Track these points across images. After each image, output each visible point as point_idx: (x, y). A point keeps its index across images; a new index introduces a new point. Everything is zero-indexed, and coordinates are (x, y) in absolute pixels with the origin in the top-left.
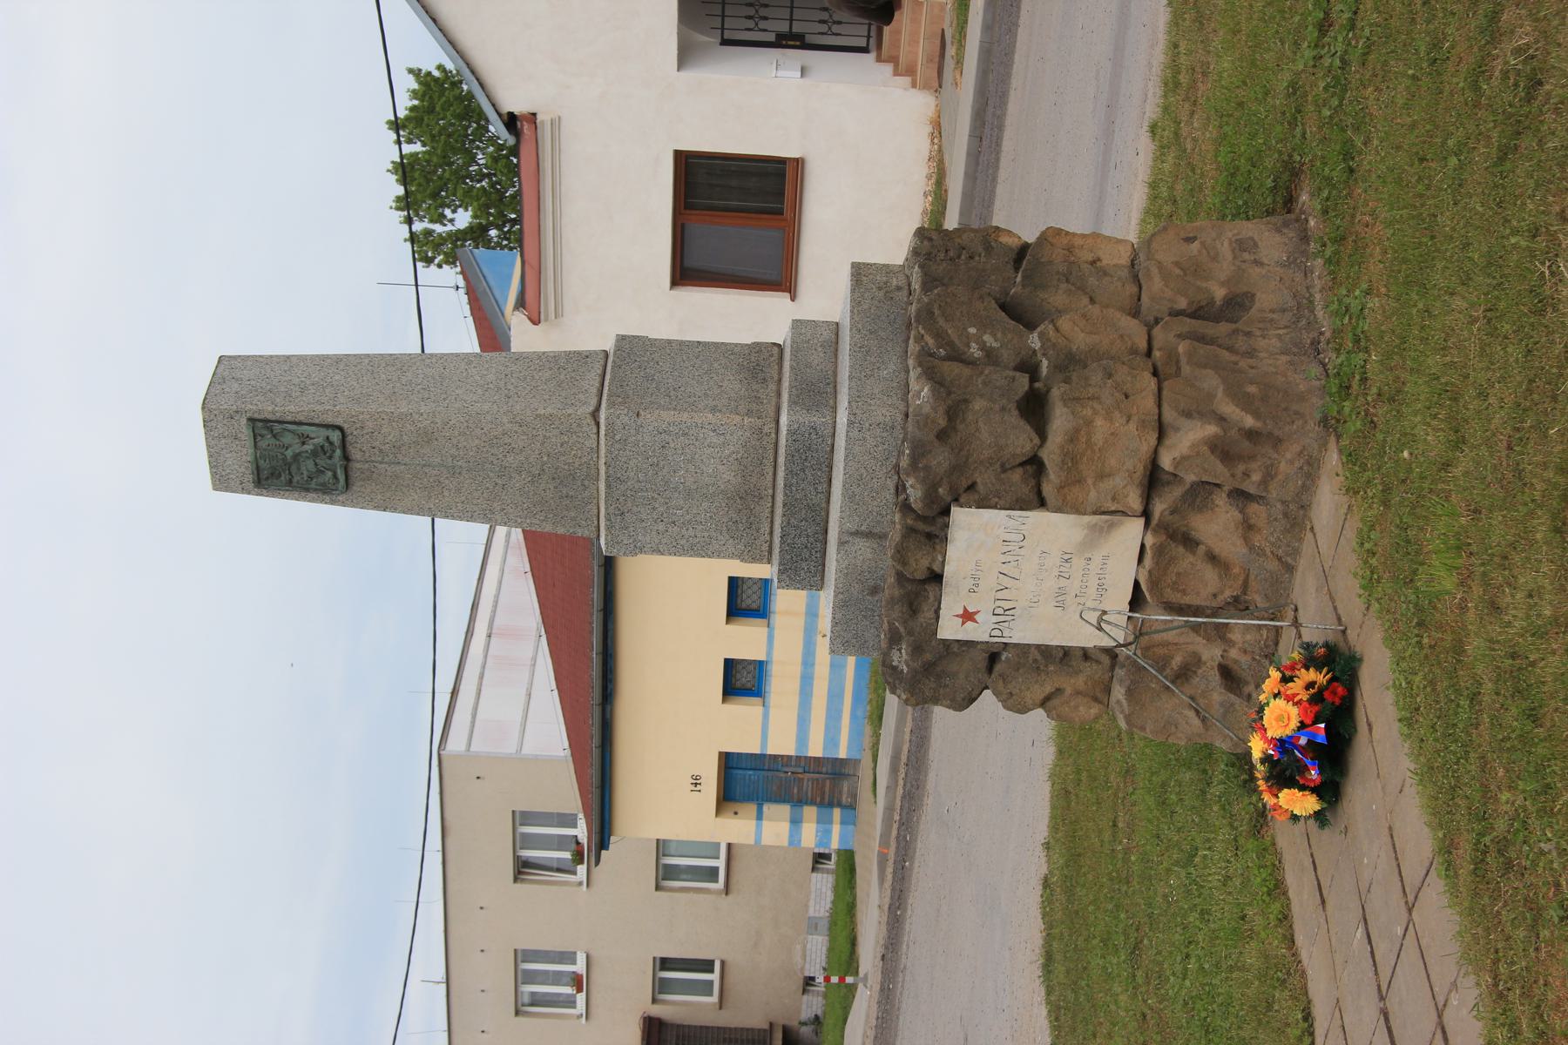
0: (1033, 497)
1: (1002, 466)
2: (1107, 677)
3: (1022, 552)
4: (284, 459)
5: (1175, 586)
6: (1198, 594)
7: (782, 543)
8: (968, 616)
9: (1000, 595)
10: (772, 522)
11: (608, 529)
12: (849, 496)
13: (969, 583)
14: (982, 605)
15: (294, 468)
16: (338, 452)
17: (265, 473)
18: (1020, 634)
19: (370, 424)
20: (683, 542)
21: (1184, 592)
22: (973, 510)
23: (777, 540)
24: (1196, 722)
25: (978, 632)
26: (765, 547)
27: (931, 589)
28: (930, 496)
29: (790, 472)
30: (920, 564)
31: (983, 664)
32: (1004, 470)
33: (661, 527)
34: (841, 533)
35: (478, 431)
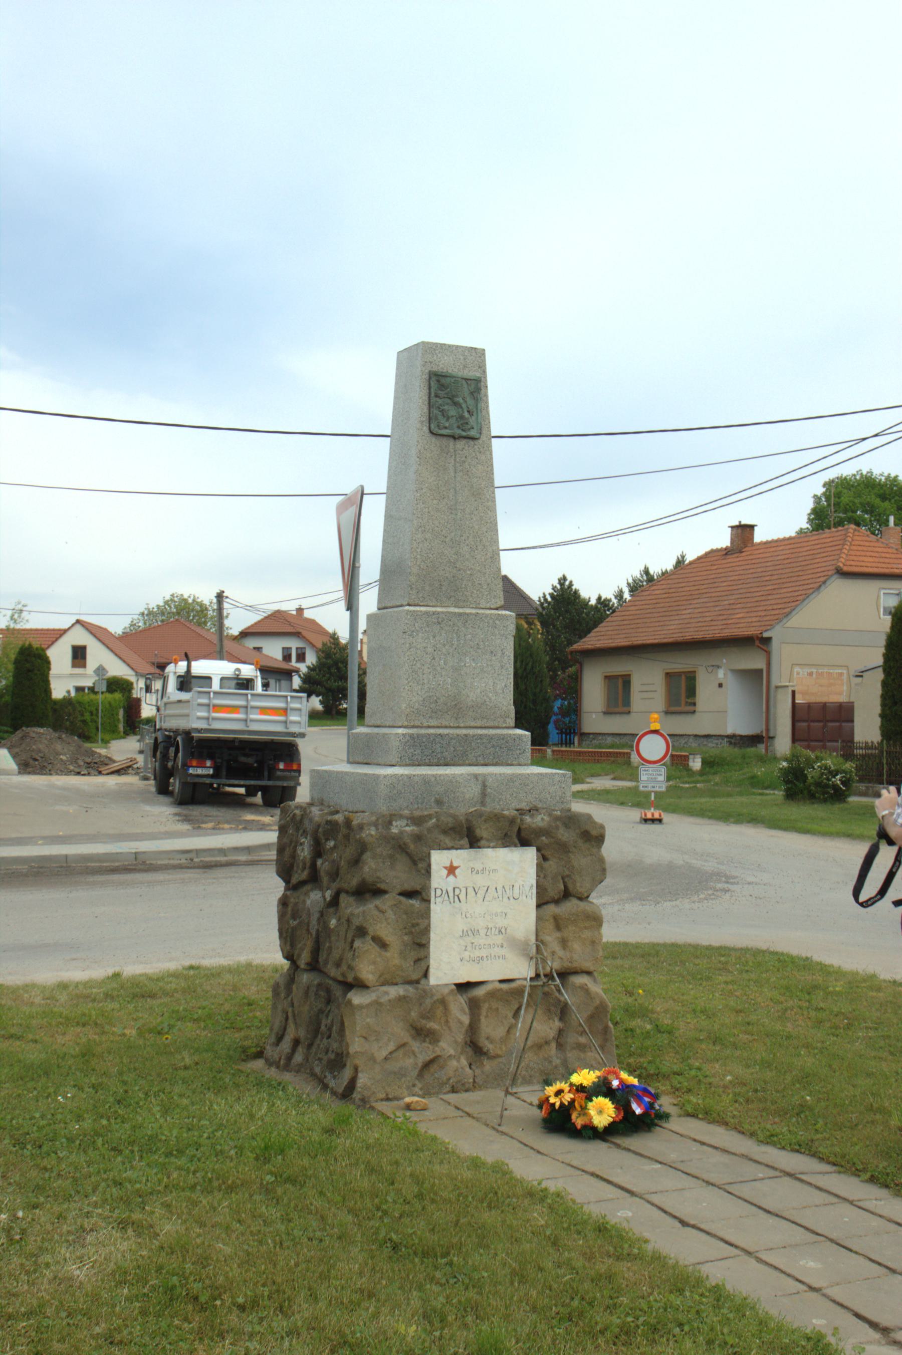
0: (546, 899)
1: (568, 876)
2: (398, 980)
3: (506, 900)
4: (457, 396)
5: (490, 1008)
6: (487, 1026)
7: (436, 735)
8: (451, 870)
9: (470, 890)
10: (438, 727)
11: (427, 613)
12: (512, 779)
13: (478, 866)
14: (462, 878)
15: (449, 401)
16: (464, 434)
17: (443, 381)
18: (439, 911)
19: (483, 457)
20: (418, 665)
21: (487, 1016)
22: (535, 862)
23: (441, 731)
24: (384, 1053)
25: (439, 879)
26: (417, 723)
27: (465, 842)
28: (541, 831)
29: (491, 738)
30: (482, 831)
31: (407, 887)
32: (563, 878)
33: (430, 650)
34: (484, 775)
35: (484, 529)
